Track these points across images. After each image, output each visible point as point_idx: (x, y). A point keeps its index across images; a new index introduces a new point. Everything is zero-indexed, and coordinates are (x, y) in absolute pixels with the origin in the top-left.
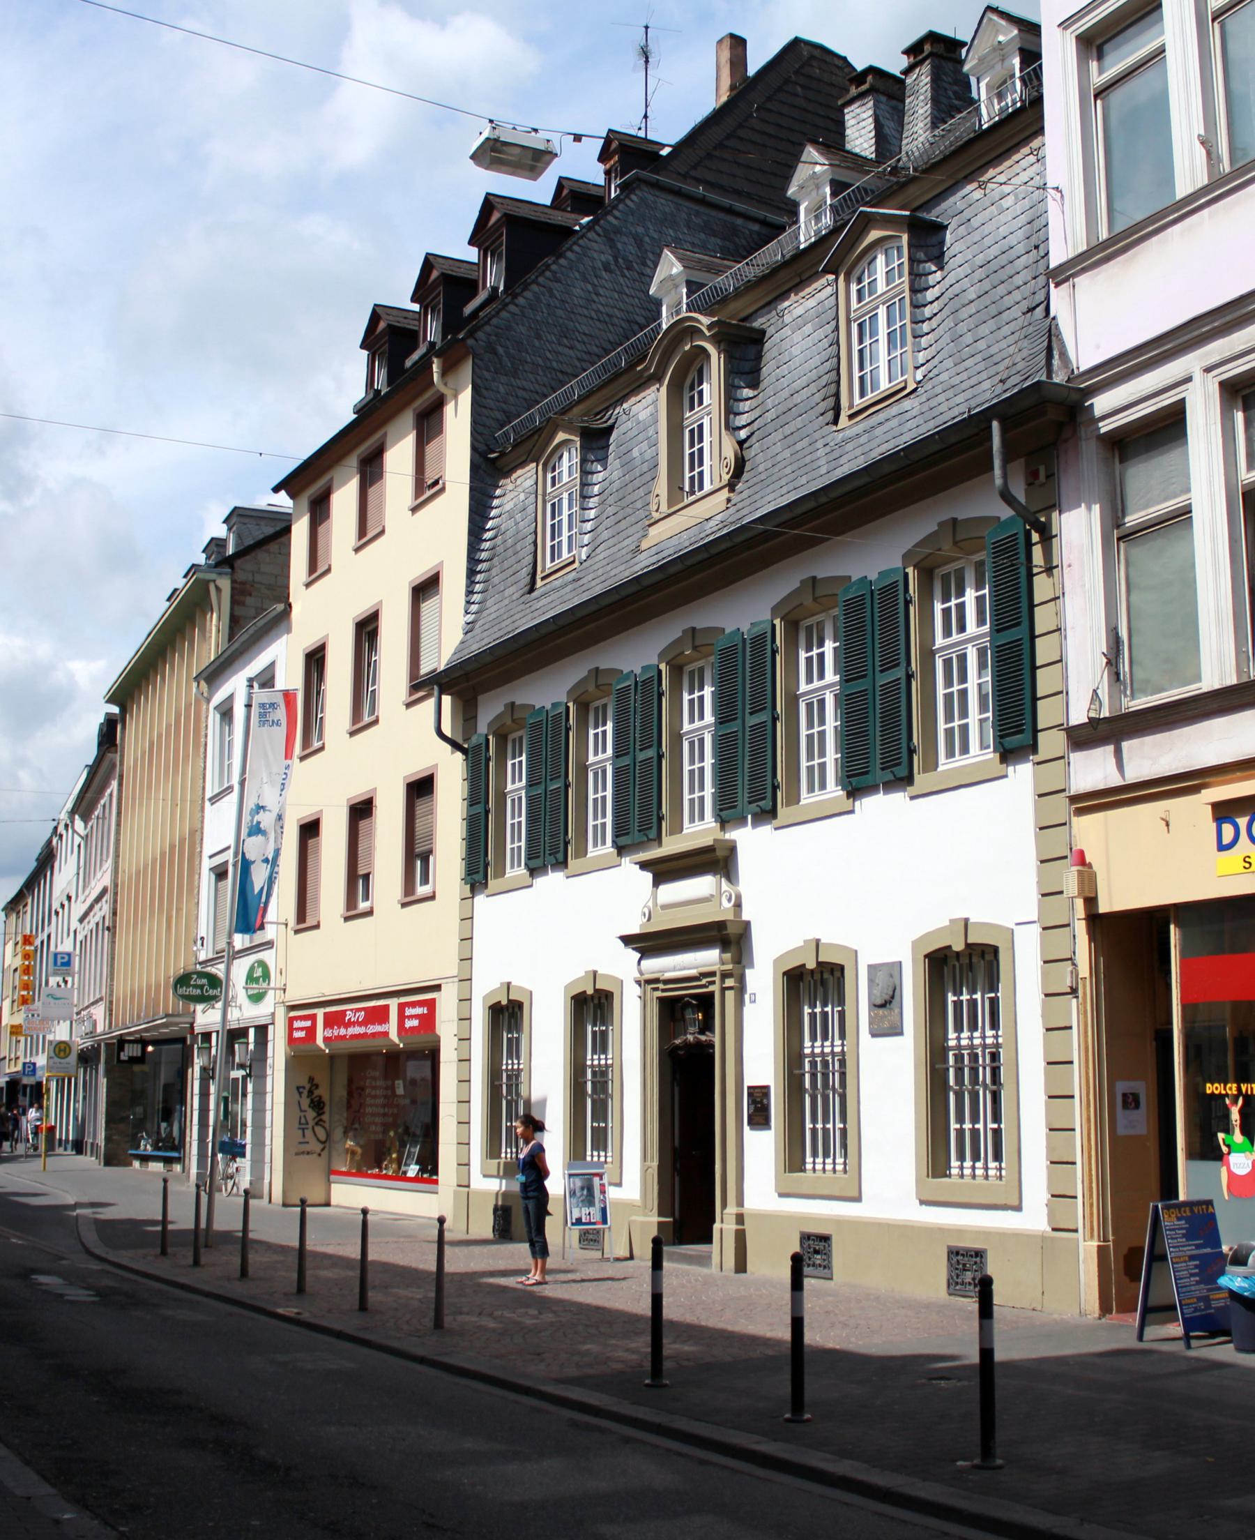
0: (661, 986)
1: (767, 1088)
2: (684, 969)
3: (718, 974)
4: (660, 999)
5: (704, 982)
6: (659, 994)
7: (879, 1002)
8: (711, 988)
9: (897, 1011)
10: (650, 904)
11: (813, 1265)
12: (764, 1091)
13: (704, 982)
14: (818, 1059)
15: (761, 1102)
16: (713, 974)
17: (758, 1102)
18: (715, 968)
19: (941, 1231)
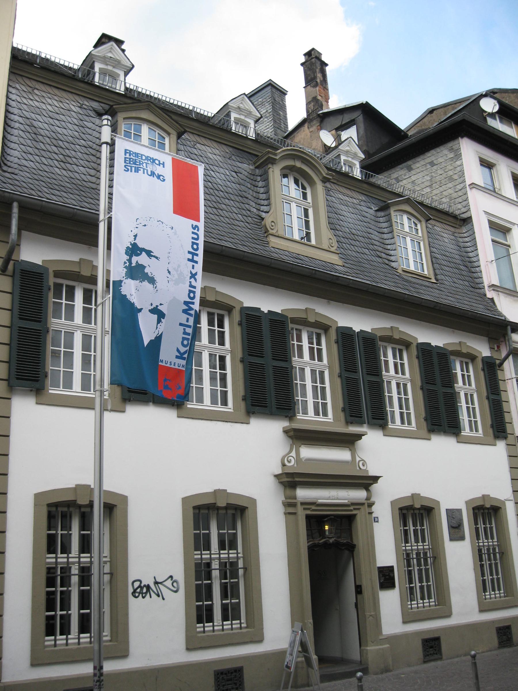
0: (313, 507)
1: (392, 567)
2: (338, 499)
3: (366, 505)
4: (308, 518)
5: (352, 508)
6: (309, 512)
7: (454, 525)
8: (354, 512)
9: (462, 529)
10: (293, 454)
11: (431, 654)
12: (390, 569)
13: (352, 508)
14: (491, 547)
15: (389, 575)
16: (363, 504)
17: (387, 576)
18: (363, 501)
19: (493, 622)
